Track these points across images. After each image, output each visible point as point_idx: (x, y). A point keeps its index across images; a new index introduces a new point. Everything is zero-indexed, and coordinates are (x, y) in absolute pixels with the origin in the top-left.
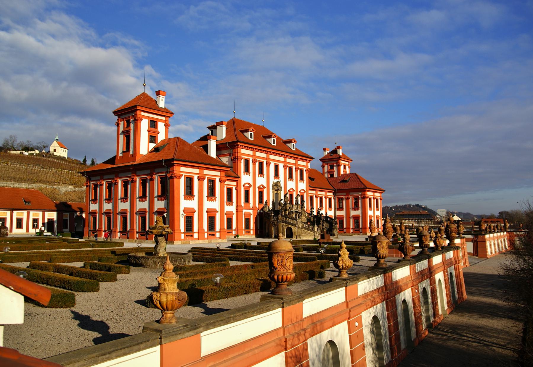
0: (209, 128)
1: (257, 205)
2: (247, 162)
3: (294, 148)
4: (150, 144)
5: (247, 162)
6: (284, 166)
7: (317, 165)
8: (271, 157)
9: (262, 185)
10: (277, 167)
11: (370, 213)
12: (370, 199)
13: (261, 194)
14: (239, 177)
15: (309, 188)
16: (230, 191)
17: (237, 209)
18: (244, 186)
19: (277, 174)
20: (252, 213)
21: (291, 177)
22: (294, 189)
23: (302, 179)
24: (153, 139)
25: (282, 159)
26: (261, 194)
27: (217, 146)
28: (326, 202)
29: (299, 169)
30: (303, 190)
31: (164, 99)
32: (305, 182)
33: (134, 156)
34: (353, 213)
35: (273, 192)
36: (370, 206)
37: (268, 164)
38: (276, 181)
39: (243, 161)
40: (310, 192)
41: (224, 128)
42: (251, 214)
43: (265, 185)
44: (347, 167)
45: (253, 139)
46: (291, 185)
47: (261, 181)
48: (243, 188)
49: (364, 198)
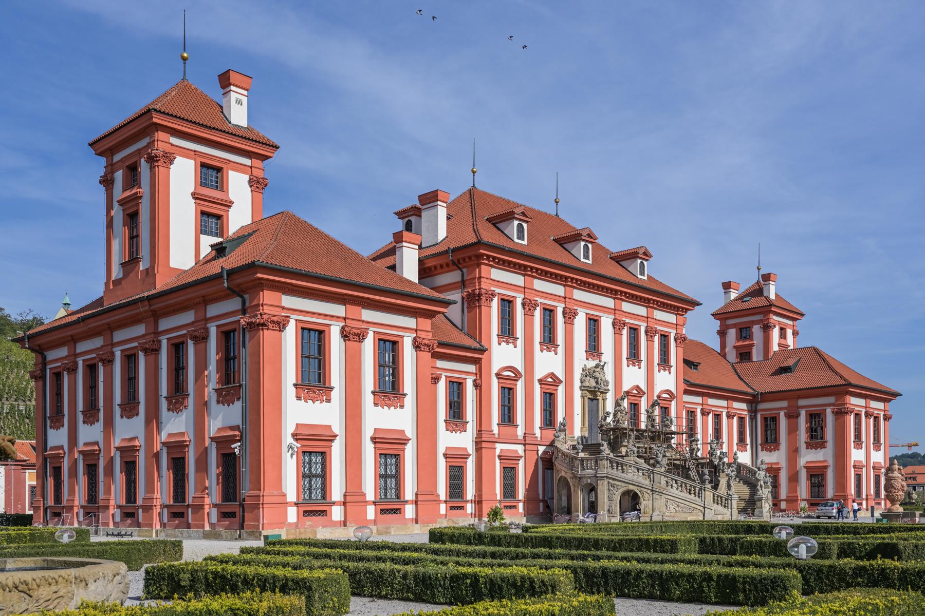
0: (401, 214)
1: (538, 433)
2: (507, 304)
3: (642, 273)
4: (203, 238)
5: (507, 304)
6: (614, 324)
7: (702, 328)
8: (579, 295)
9: (552, 375)
10: (593, 324)
11: (856, 455)
12: (857, 416)
13: (549, 399)
14: (482, 351)
15: (683, 386)
16: (456, 387)
17: (479, 444)
18: (497, 375)
19: (594, 348)
20: (521, 453)
21: (634, 356)
22: (643, 387)
23: (665, 362)
24: (211, 217)
25: (609, 302)
26: (549, 399)
27: (421, 261)
28: (730, 428)
29: (656, 332)
30: (668, 392)
31: (245, 100)
32: (673, 370)
33: (150, 273)
34: (808, 457)
35: (583, 397)
36: (858, 436)
37: (570, 315)
38: (591, 364)
39: (495, 303)
40: (687, 398)
41: (442, 212)
42: (518, 458)
43: (560, 375)
44: (789, 332)
45: (525, 243)
46: (633, 377)
47: (548, 363)
48: (495, 382)
49: (841, 413)
